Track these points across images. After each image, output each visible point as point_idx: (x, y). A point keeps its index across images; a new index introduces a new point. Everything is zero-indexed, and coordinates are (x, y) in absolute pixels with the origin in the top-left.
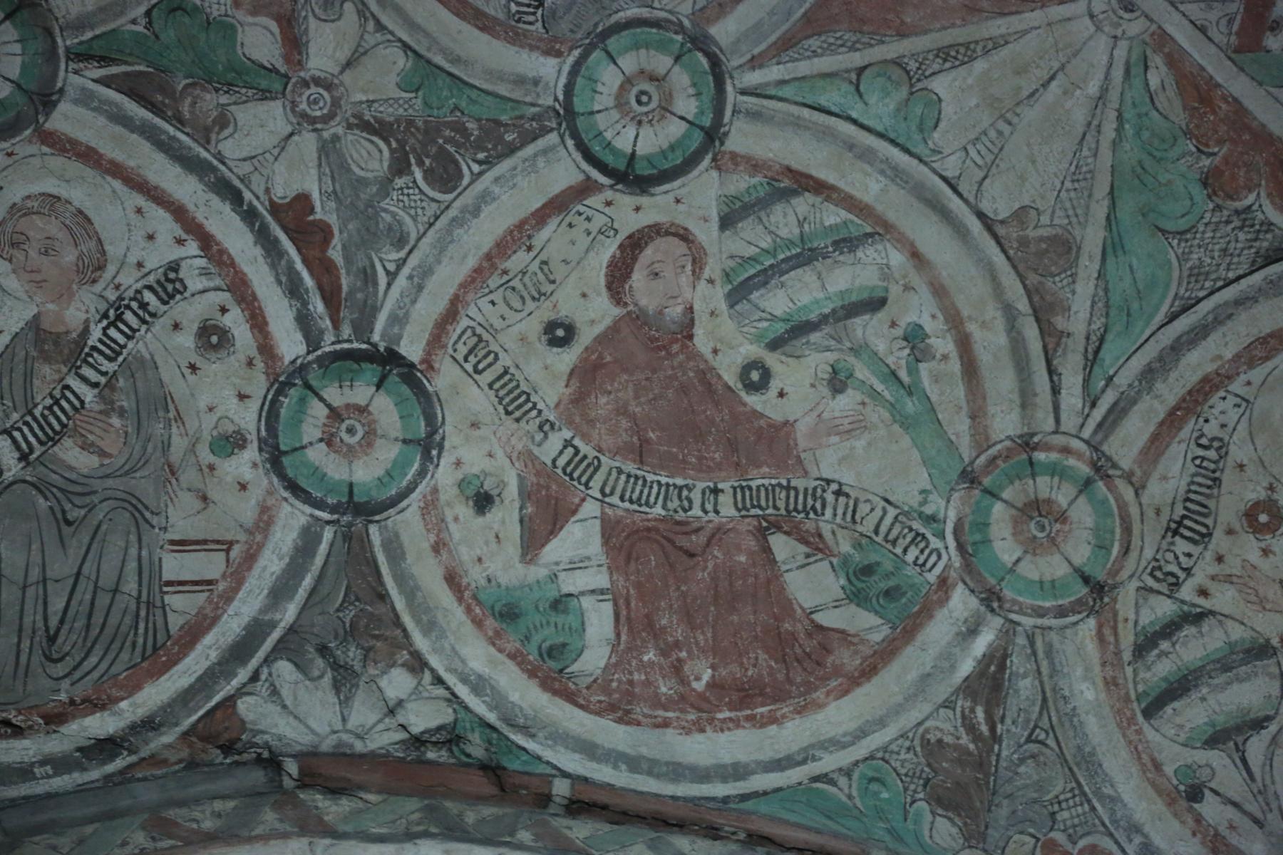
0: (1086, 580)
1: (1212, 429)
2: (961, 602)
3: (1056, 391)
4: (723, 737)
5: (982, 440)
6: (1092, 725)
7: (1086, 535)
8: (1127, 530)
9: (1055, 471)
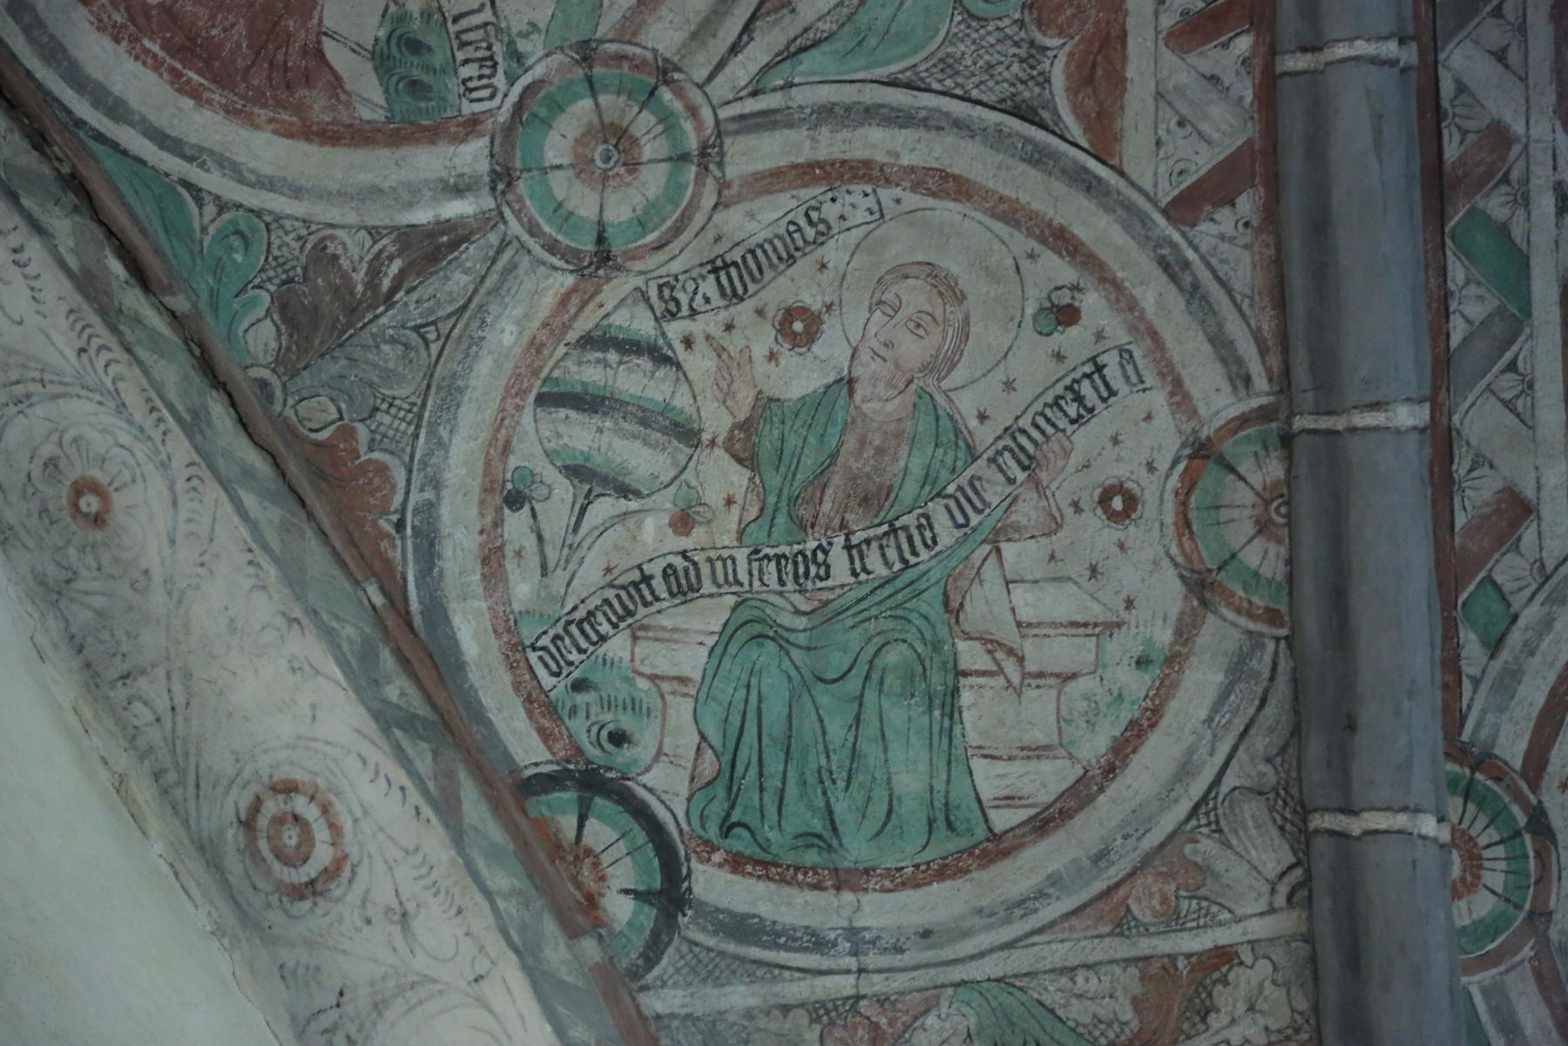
0: (601, 239)
1: (830, 211)
2: (472, 155)
3: (735, 49)
4: (132, 65)
5: (629, 30)
6: (484, 366)
7: (638, 200)
8: (677, 230)
9: (667, 121)
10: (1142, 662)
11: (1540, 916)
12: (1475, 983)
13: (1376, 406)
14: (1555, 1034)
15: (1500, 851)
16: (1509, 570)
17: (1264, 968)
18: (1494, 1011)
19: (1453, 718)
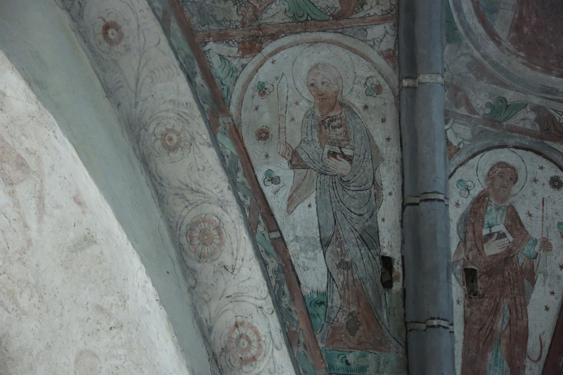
14: (473, 12)
18: (455, 4)
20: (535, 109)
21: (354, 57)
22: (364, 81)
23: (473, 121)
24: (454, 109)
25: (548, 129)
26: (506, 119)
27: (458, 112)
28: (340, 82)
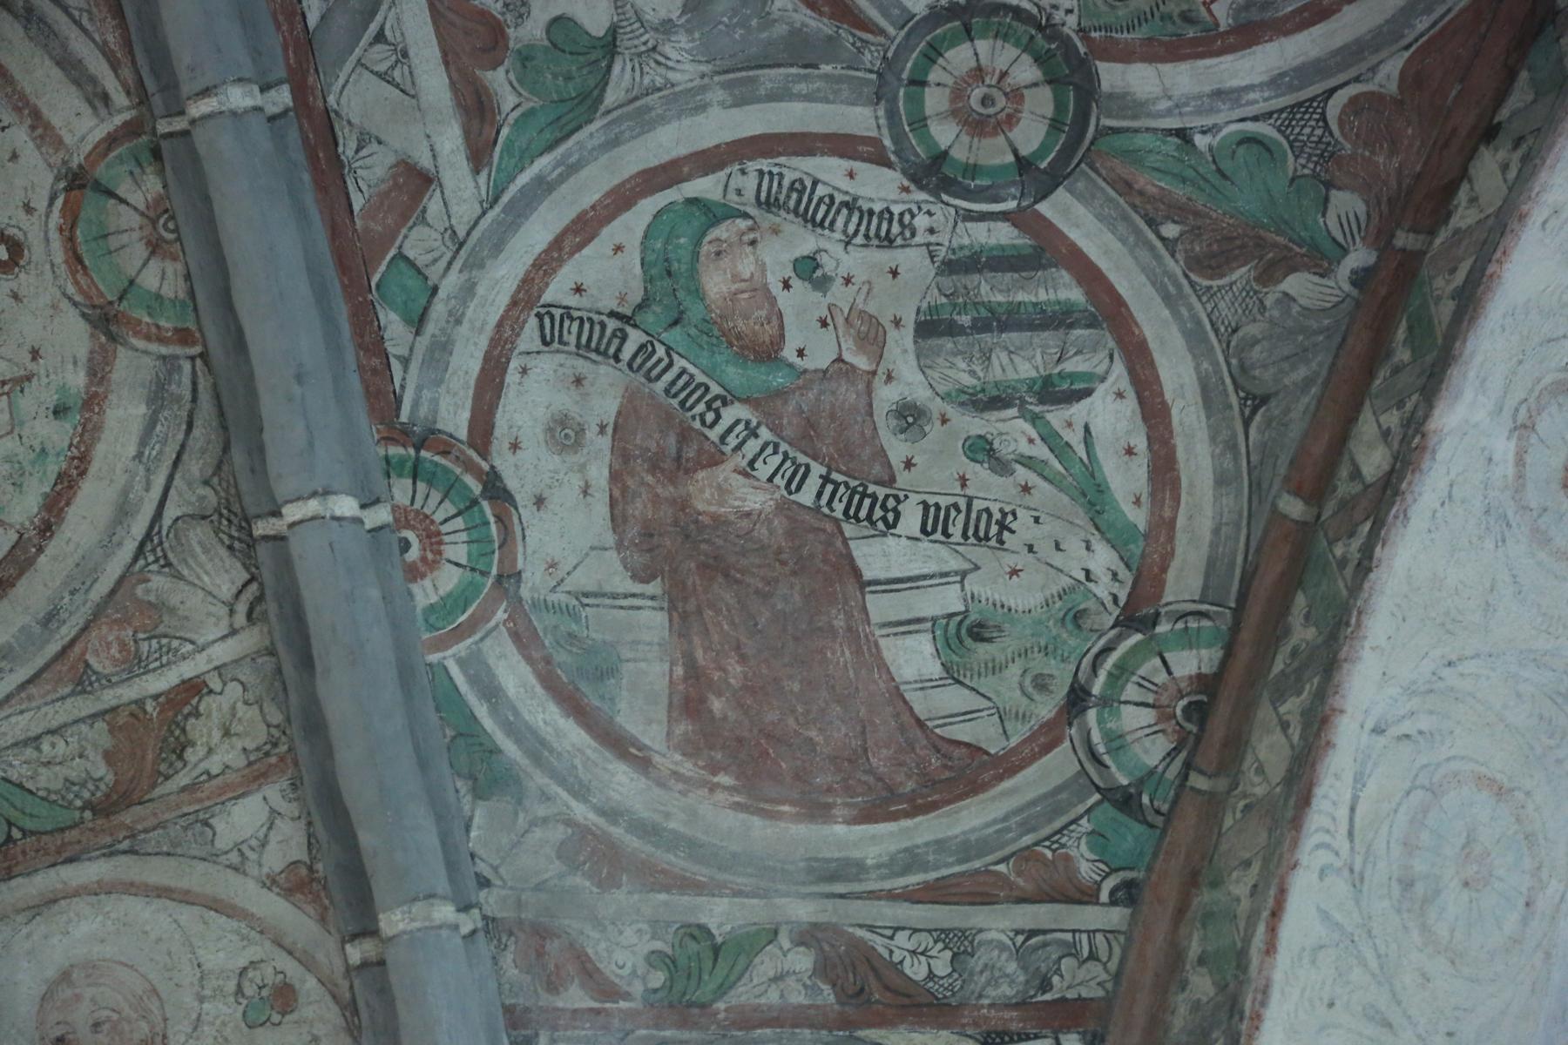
10: (59, 412)
11: (509, 578)
12: (450, 659)
13: (206, 92)
14: (539, 690)
15: (459, 523)
16: (419, 243)
17: (234, 690)
18: (473, 681)
19: (383, 401)
20: (808, 936)
21: (187, 914)
22: (231, 986)
23: (616, 1022)
24: (546, 999)
25: (862, 990)
26: (722, 990)
27: (560, 1004)
28: (154, 1005)
